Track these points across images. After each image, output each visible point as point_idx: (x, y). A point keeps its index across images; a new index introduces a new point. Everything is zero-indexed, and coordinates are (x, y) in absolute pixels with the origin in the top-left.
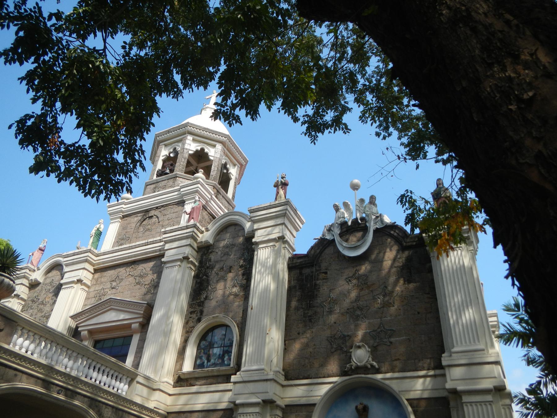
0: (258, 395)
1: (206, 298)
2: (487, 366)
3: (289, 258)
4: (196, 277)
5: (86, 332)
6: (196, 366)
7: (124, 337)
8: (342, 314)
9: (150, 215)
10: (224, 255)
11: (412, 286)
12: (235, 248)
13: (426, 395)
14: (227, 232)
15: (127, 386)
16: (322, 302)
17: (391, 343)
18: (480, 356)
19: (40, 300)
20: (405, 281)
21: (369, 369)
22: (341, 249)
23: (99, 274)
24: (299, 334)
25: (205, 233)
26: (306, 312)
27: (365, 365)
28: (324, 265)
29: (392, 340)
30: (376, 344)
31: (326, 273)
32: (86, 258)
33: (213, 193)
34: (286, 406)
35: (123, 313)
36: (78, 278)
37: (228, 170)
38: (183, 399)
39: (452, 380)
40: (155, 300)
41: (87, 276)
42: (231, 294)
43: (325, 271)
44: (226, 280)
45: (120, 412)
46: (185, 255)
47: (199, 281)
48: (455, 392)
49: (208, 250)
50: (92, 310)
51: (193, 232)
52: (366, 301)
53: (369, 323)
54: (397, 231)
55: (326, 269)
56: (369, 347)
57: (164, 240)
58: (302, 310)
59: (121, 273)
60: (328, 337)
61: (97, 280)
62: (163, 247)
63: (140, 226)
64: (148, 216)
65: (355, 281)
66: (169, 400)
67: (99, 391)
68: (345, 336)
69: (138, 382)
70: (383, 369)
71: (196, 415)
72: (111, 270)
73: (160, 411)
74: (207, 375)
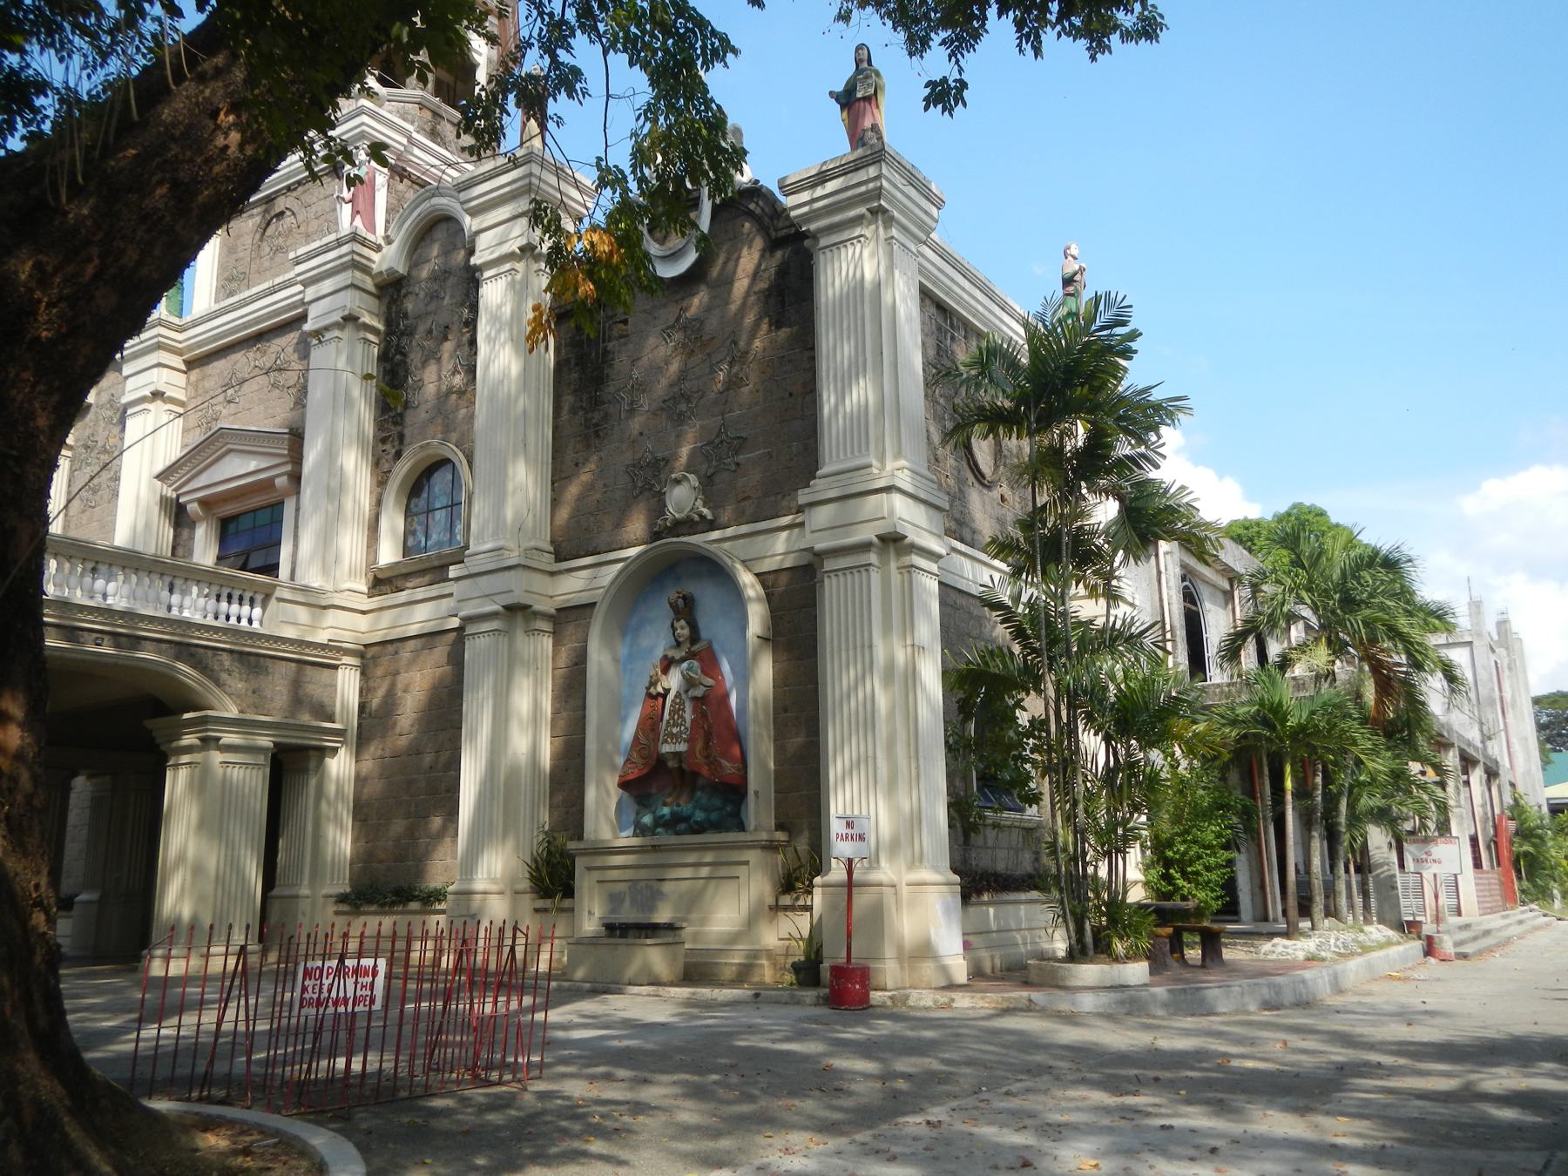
0: (495, 598)
4: (383, 357)
5: (195, 505)
6: (406, 551)
7: (272, 506)
8: (654, 414)
9: (277, 210)
10: (432, 298)
11: (783, 333)
12: (452, 280)
13: (787, 565)
14: (433, 241)
15: (257, 611)
16: (619, 390)
17: (738, 464)
18: (863, 479)
19: (100, 444)
20: (770, 325)
21: (697, 523)
23: (197, 370)
24: (577, 465)
25: (386, 249)
26: (589, 415)
29: (741, 458)
31: (625, 322)
32: (155, 340)
33: (410, 128)
34: (558, 610)
35: (252, 456)
36: (152, 388)
38: (387, 618)
39: (813, 532)
40: (303, 421)
41: (174, 382)
42: (450, 391)
44: (439, 360)
45: (252, 658)
46: (346, 313)
47: (388, 366)
48: (820, 556)
49: (399, 291)
50: (194, 457)
51: (353, 252)
52: (697, 378)
53: (702, 427)
54: (761, 203)
56: (699, 478)
57: (299, 279)
58: (581, 413)
59: (238, 365)
60: (628, 466)
61: (196, 388)
62: (300, 296)
63: (261, 240)
64: (273, 213)
65: (678, 336)
66: (363, 623)
67: (189, 628)
68: (657, 461)
69: (280, 600)
70: (724, 518)
71: (411, 644)
72: (217, 360)
73: (344, 645)
74: (419, 567)
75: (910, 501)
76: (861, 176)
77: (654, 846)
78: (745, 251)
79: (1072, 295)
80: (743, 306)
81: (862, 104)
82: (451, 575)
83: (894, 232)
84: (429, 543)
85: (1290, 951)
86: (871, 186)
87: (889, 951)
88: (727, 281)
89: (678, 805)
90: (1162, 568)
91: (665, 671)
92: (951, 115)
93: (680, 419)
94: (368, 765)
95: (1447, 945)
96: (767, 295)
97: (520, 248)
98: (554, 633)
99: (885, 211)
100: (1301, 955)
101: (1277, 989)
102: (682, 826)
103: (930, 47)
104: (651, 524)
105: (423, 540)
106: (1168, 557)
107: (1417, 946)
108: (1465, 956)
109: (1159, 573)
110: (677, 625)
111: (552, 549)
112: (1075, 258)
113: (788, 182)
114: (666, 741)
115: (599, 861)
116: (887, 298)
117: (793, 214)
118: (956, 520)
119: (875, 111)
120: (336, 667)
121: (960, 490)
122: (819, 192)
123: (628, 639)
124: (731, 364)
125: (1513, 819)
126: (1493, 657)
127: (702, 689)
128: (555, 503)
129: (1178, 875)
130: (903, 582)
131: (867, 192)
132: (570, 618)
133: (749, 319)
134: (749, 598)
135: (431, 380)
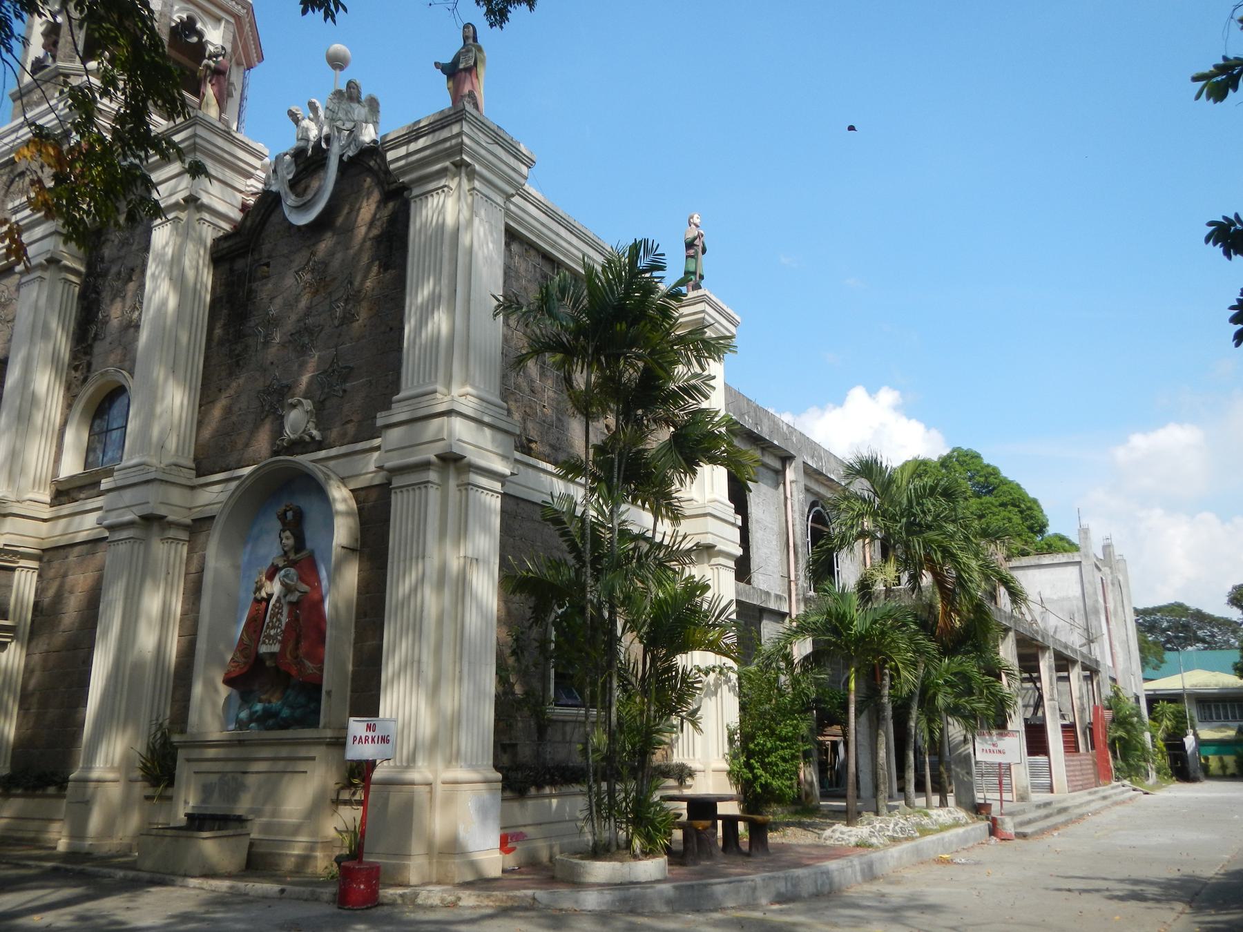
1: (95, 339)
2: (436, 422)
3: (216, 241)
4: (83, 296)
6: (86, 466)
9: (19, 170)
13: (376, 482)
16: (257, 325)
17: (345, 391)
18: (428, 403)
20: (379, 268)
22: (287, 212)
24: (220, 390)
27: (301, 437)
28: (266, 247)
30: (323, 397)
31: (268, 265)
37: (200, 35)
43: (266, 261)
44: (124, 298)
46: (49, 256)
54: (378, 160)
55: (269, 257)
56: (314, 403)
58: (227, 345)
60: (259, 392)
64: (16, 173)
71: (77, 550)
75: (472, 424)
76: (445, 134)
77: (239, 741)
78: (365, 204)
79: (692, 257)
80: (361, 249)
81: (463, 73)
82: (103, 487)
83: (477, 184)
84: (105, 459)
85: (845, 837)
86: (454, 142)
87: (417, 848)
88: (349, 229)
90: (789, 495)
91: (271, 577)
92: (334, 22)
93: (303, 351)
94: (36, 658)
95: (1009, 826)
96: (378, 240)
97: (183, 199)
98: (189, 541)
99: (469, 165)
100: (853, 840)
101: (796, 882)
102: (271, 722)
103: (508, 19)
104: (273, 444)
105: (101, 456)
106: (794, 485)
107: (983, 825)
108: (1024, 836)
109: (786, 498)
110: (283, 535)
111: (193, 466)
112: (697, 226)
113: (388, 139)
114: (264, 642)
115: (195, 753)
116: (465, 239)
117: (392, 167)
118: (553, 447)
119: (474, 80)
120: (13, 569)
121: (559, 419)
122: (413, 147)
123: (249, 547)
124: (346, 302)
125: (1110, 709)
126: (1098, 575)
127: (297, 594)
128: (200, 424)
129: (757, 765)
130: (461, 496)
131: (451, 147)
132: (198, 527)
133: (365, 259)
134: (338, 513)
135: (115, 313)
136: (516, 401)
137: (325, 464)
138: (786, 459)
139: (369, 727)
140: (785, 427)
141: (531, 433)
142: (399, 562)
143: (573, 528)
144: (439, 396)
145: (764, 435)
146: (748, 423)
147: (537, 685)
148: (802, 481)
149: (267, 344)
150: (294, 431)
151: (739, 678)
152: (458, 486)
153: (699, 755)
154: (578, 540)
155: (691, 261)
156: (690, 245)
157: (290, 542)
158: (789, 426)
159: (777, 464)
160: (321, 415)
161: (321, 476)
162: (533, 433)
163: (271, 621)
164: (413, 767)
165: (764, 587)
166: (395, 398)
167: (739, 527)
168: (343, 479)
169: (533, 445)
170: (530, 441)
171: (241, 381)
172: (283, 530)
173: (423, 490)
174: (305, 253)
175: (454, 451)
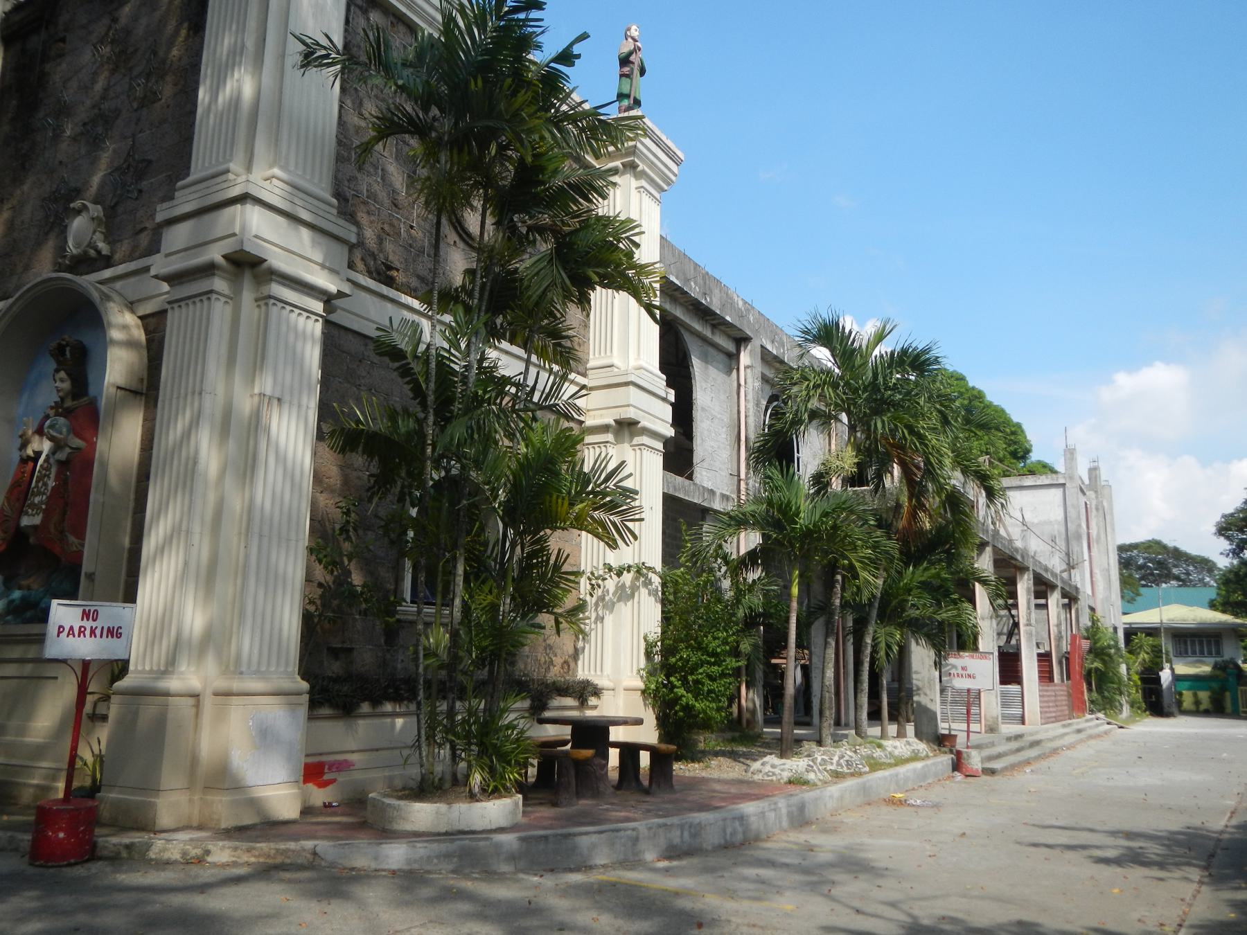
17: (140, 191)
18: (219, 187)
20: (189, 30)
27: (85, 252)
29: (144, 184)
31: (63, 40)
56: (104, 209)
60: (44, 199)
79: (627, 76)
85: (777, 771)
87: (171, 777)
89: (29, 588)
90: (742, 382)
95: (975, 760)
100: (786, 775)
101: (697, 830)
102: (29, 614)
106: (749, 371)
107: (946, 759)
108: (992, 772)
109: (739, 385)
112: (635, 40)
114: (27, 513)
118: (419, 277)
123: (25, 397)
125: (1087, 638)
126: (1082, 499)
127: (68, 450)
129: (678, 684)
136: (368, 213)
137: (111, 285)
138: (741, 340)
139: (86, 615)
140: (741, 303)
141: (391, 258)
142: (171, 399)
143: (417, 367)
144: (231, 176)
145: (713, 308)
146: (694, 291)
147: (384, 573)
148: (759, 368)
149: (57, 137)
150: (77, 245)
151: (664, 585)
152: (256, 300)
153: (608, 669)
154: (421, 380)
155: (626, 81)
156: (625, 61)
157: (66, 385)
158: (745, 303)
159: (730, 347)
160: (110, 224)
161: (95, 296)
162: (395, 260)
163: (37, 486)
164: (172, 673)
165: (708, 485)
166: (180, 184)
167: (672, 404)
168: (132, 303)
169: (395, 273)
170: (390, 268)
171: (26, 187)
172: (57, 371)
173: (206, 302)
174: (106, 21)
175: (247, 248)
